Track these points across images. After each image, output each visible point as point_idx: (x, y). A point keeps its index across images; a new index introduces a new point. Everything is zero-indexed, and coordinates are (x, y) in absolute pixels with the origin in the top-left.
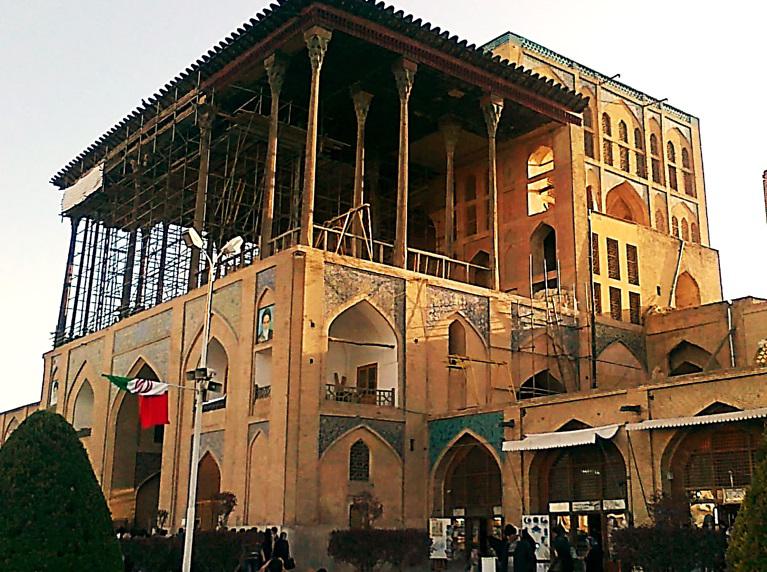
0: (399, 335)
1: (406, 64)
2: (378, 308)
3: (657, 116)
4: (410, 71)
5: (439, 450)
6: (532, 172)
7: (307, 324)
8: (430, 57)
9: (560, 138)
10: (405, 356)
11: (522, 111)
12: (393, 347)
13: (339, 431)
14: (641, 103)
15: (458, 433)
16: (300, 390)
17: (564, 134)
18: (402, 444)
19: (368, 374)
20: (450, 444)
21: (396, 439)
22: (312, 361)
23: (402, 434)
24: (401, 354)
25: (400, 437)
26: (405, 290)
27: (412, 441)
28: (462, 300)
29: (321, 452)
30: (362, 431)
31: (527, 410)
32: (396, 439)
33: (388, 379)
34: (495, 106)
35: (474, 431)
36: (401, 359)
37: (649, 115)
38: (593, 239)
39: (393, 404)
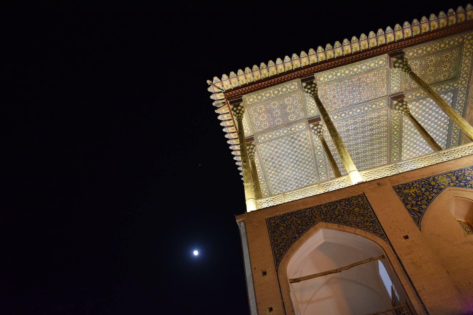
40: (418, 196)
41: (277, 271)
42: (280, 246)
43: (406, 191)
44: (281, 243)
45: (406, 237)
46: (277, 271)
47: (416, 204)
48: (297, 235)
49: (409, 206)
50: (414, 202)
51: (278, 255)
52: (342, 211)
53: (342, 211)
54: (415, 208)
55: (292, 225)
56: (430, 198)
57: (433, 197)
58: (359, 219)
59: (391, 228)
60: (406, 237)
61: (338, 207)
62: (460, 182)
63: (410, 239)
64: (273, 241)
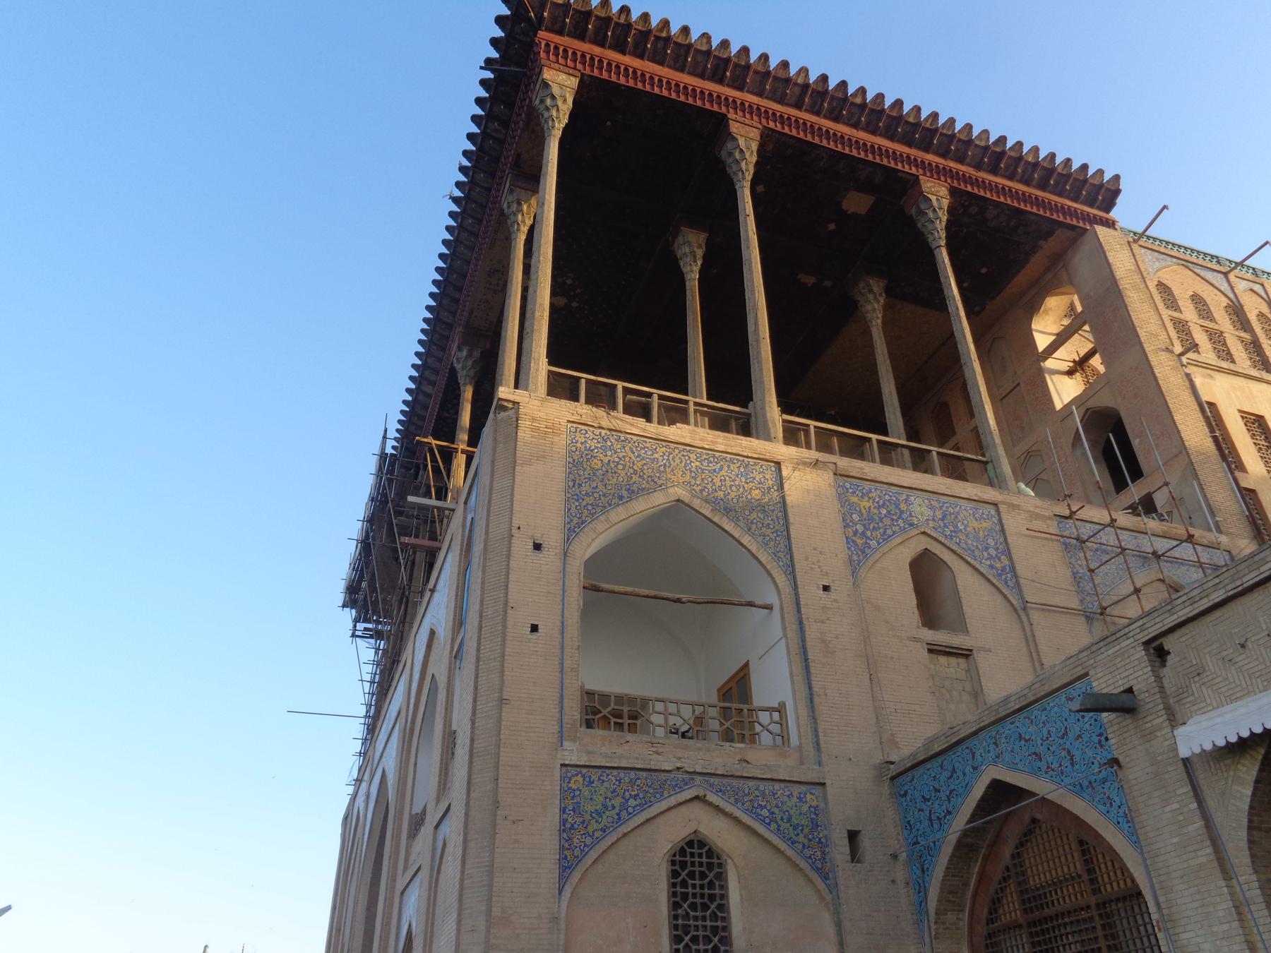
0: (781, 579)
1: (734, 128)
2: (716, 519)
3: (1257, 288)
4: (747, 139)
5: (932, 850)
6: (1042, 342)
7: (521, 546)
8: (782, 119)
9: (1080, 262)
10: (801, 623)
11: (991, 212)
12: (769, 607)
13: (624, 806)
14: (1224, 270)
15: (968, 787)
16: (502, 701)
17: (1085, 248)
18: (823, 844)
19: (737, 688)
20: (960, 822)
21: (813, 845)
22: (534, 628)
23: (816, 821)
24: (791, 618)
25: (815, 825)
26: (781, 486)
27: (853, 836)
28: (931, 507)
29: (566, 866)
30: (697, 806)
31: (1169, 643)
32: (813, 845)
33: (774, 684)
34: (933, 198)
35: (1013, 767)
36: (793, 634)
37: (1241, 286)
38: (1211, 416)
39: (784, 737)
40: (871, 519)
41: (565, 554)
42: (584, 503)
43: (855, 499)
44: (587, 494)
45: (826, 588)
46: (565, 554)
47: (863, 533)
48: (625, 493)
49: (850, 532)
50: (860, 528)
51: (575, 520)
52: (728, 483)
53: (728, 483)
54: (859, 541)
55: (620, 467)
56: (889, 532)
57: (894, 533)
58: (754, 515)
59: (807, 559)
60: (826, 588)
61: (723, 472)
62: (945, 526)
63: (832, 595)
64: (571, 484)
